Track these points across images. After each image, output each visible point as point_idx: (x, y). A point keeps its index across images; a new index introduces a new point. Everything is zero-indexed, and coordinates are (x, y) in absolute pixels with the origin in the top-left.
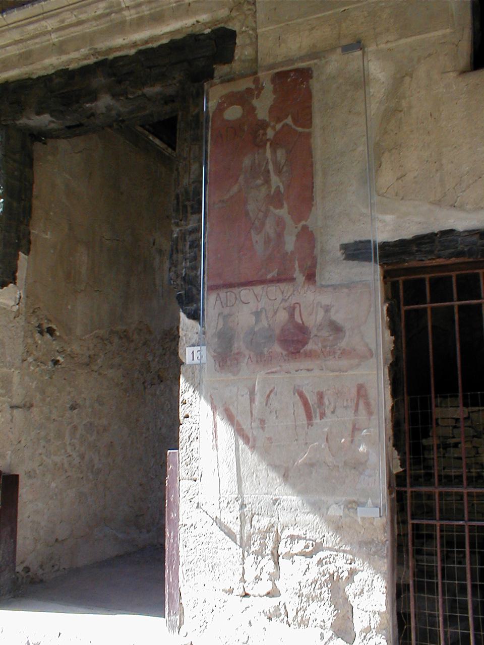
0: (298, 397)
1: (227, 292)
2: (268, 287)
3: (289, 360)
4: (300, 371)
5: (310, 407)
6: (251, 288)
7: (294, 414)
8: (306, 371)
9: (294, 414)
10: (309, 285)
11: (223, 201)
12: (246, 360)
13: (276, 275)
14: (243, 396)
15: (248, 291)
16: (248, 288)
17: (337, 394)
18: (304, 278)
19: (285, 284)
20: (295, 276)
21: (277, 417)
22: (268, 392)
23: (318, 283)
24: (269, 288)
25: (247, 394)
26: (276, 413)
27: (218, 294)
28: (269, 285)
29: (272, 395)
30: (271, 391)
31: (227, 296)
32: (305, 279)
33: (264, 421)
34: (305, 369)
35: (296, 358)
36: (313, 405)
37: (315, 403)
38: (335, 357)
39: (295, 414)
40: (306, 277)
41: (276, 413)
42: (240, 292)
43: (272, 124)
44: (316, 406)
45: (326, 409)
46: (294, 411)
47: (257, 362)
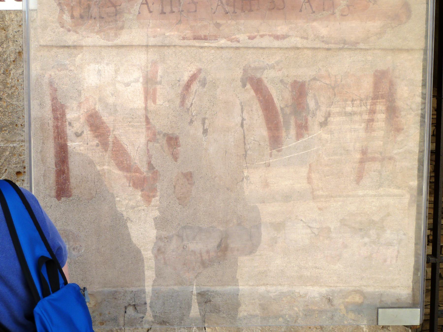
0: (253, 93)
3: (234, 12)
4: (258, 37)
5: (277, 112)
7: (242, 125)
8: (272, 38)
9: (242, 125)
12: (136, 7)
14: (128, 85)
17: (333, 88)
21: (205, 131)
22: (186, 78)
25: (137, 81)
26: (204, 123)
29: (195, 86)
30: (193, 78)
33: (177, 139)
34: (270, 36)
35: (251, 10)
36: (282, 109)
37: (287, 106)
38: (333, 14)
39: (245, 126)
41: (204, 123)
44: (288, 111)
45: (309, 118)
46: (243, 119)
47: (163, 13)
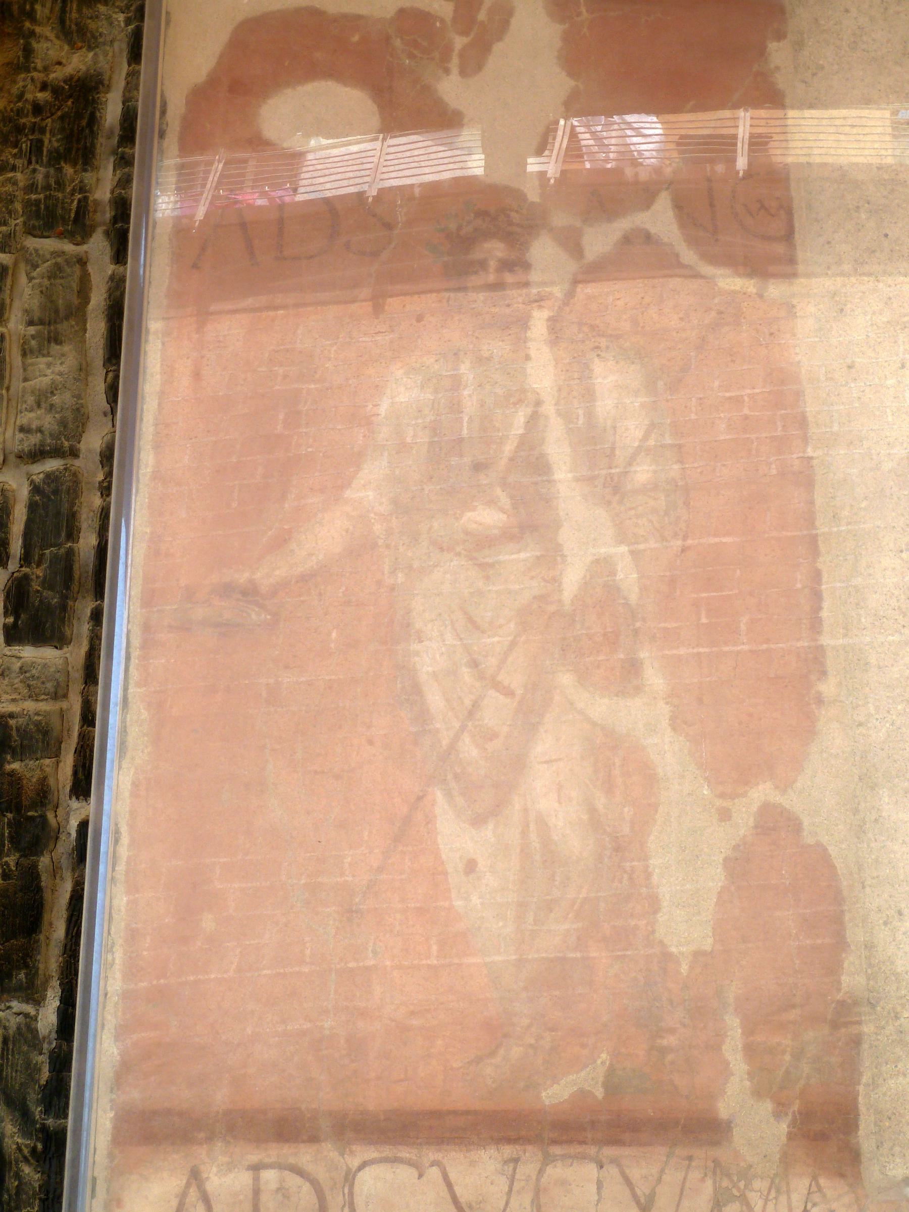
1: (256, 1168)
2: (548, 1160)
6: (431, 1154)
10: (815, 1178)
11: (250, 592)
13: (599, 1093)
15: (405, 1173)
16: (405, 1153)
18: (783, 1127)
19: (660, 1152)
20: (723, 1110)
23: (872, 1172)
24: (550, 1170)
27: (195, 1176)
28: (557, 1150)
31: (257, 1192)
32: (790, 1137)
40: (793, 1124)
42: (350, 1178)
43: (560, 219)
